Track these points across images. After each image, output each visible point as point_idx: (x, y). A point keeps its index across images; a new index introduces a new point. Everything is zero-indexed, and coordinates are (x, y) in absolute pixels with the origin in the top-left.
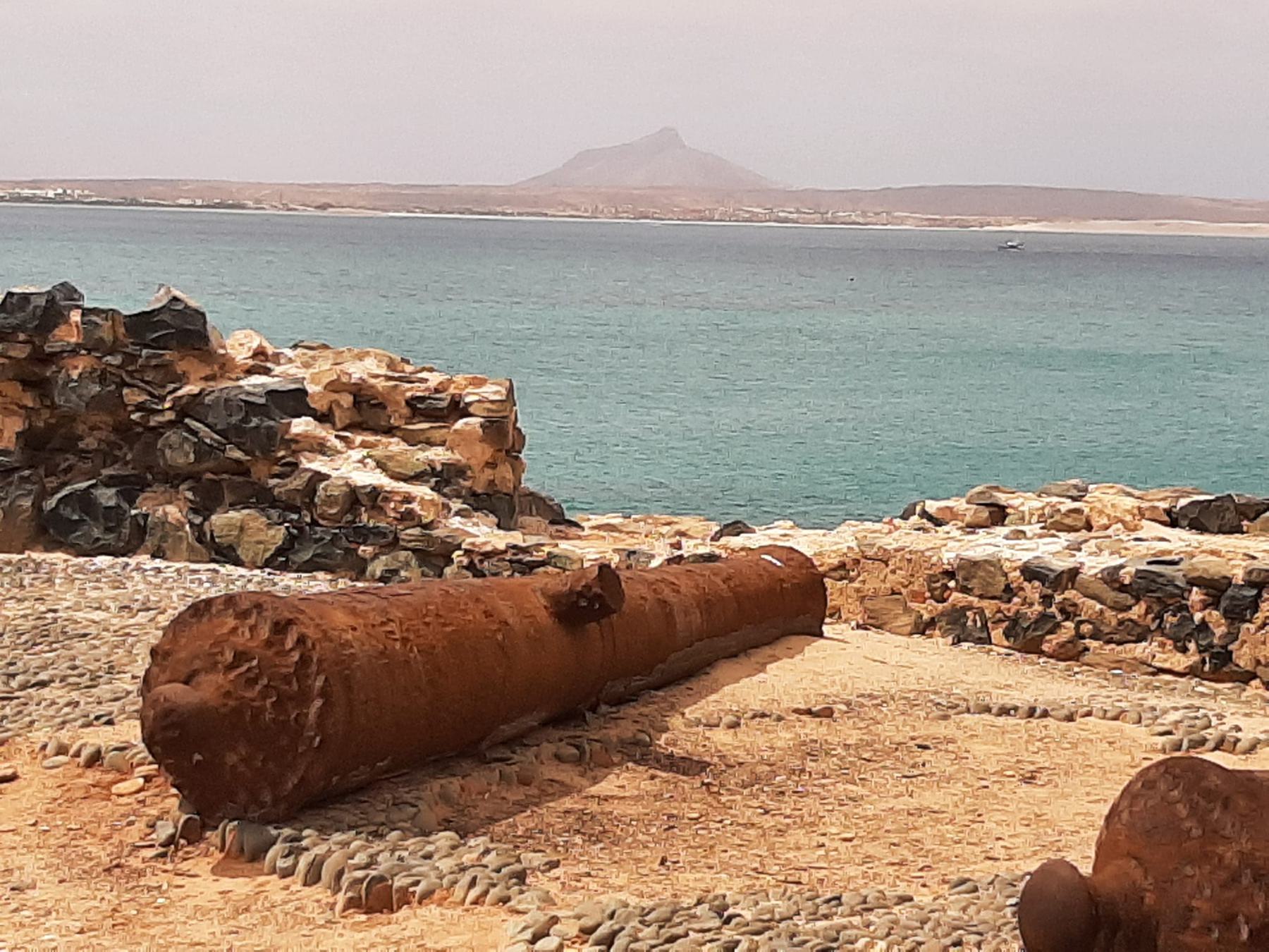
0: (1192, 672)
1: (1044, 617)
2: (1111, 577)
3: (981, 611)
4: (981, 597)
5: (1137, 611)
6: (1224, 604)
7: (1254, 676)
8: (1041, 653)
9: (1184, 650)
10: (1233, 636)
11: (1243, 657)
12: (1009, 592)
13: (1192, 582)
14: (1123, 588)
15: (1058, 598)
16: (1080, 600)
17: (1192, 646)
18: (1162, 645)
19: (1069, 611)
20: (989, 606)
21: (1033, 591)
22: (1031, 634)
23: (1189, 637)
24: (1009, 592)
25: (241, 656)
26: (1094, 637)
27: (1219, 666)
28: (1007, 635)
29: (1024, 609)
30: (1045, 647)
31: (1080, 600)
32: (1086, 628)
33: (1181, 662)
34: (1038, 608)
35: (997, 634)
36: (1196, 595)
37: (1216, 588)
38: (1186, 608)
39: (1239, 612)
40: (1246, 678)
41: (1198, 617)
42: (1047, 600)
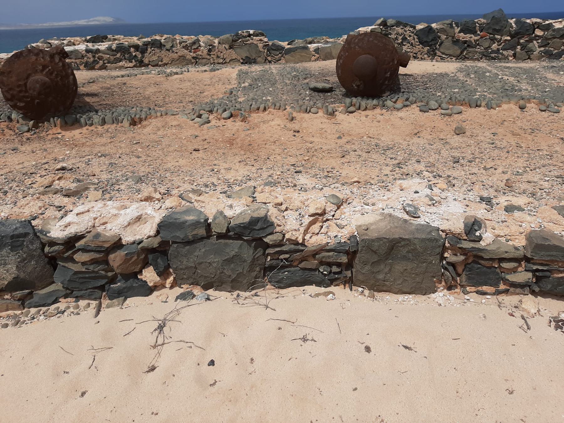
0: (134, 66)
1: (94, 61)
2: (110, 48)
3: (76, 63)
4: (75, 59)
5: (118, 55)
6: (140, 50)
7: (149, 64)
8: (95, 69)
9: (132, 62)
10: (143, 57)
11: (146, 61)
12: (83, 57)
13: (130, 47)
14: (113, 51)
15: (97, 56)
16: (103, 55)
17: (134, 61)
18: (126, 62)
19: (100, 58)
20: (78, 61)
21: (90, 55)
22: (91, 65)
23: (133, 58)
24: (83, 57)
25: (44, 67)
26: (108, 63)
27: (141, 64)
28: (85, 67)
29: (88, 60)
30: (96, 68)
31: (103, 55)
32: (106, 62)
33: (131, 65)
34: (92, 59)
35: (82, 67)
36: (132, 50)
37: (136, 47)
38: (131, 53)
39: (143, 52)
40: (147, 65)
41: (134, 54)
42: (94, 57)
